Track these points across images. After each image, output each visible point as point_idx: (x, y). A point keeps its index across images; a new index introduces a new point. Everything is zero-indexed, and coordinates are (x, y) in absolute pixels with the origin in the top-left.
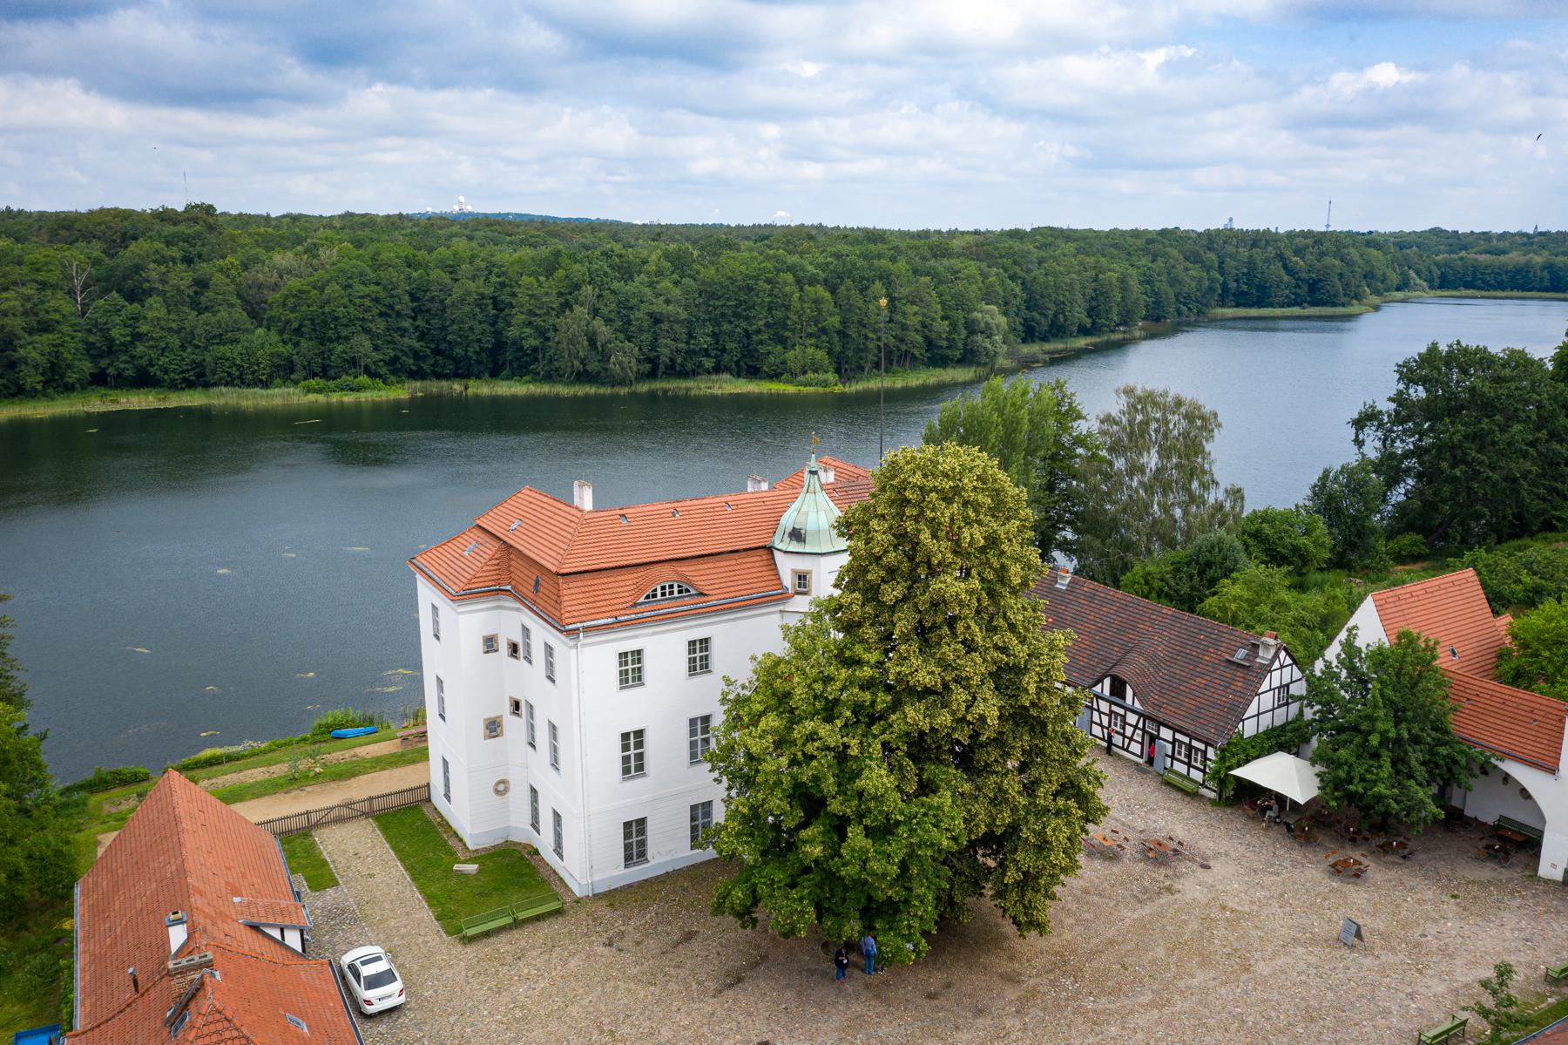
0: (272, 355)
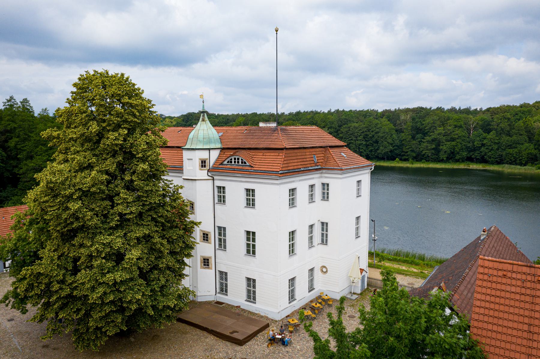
0: (528, 154)
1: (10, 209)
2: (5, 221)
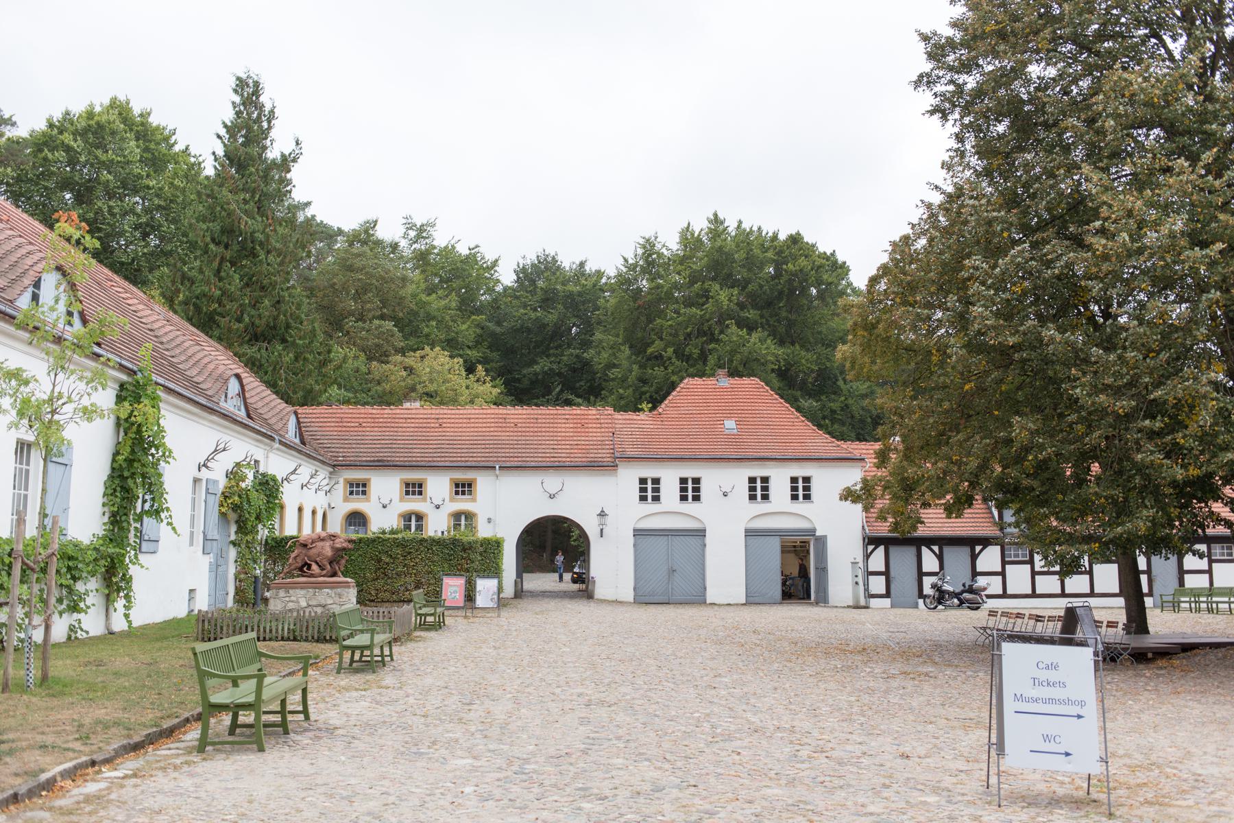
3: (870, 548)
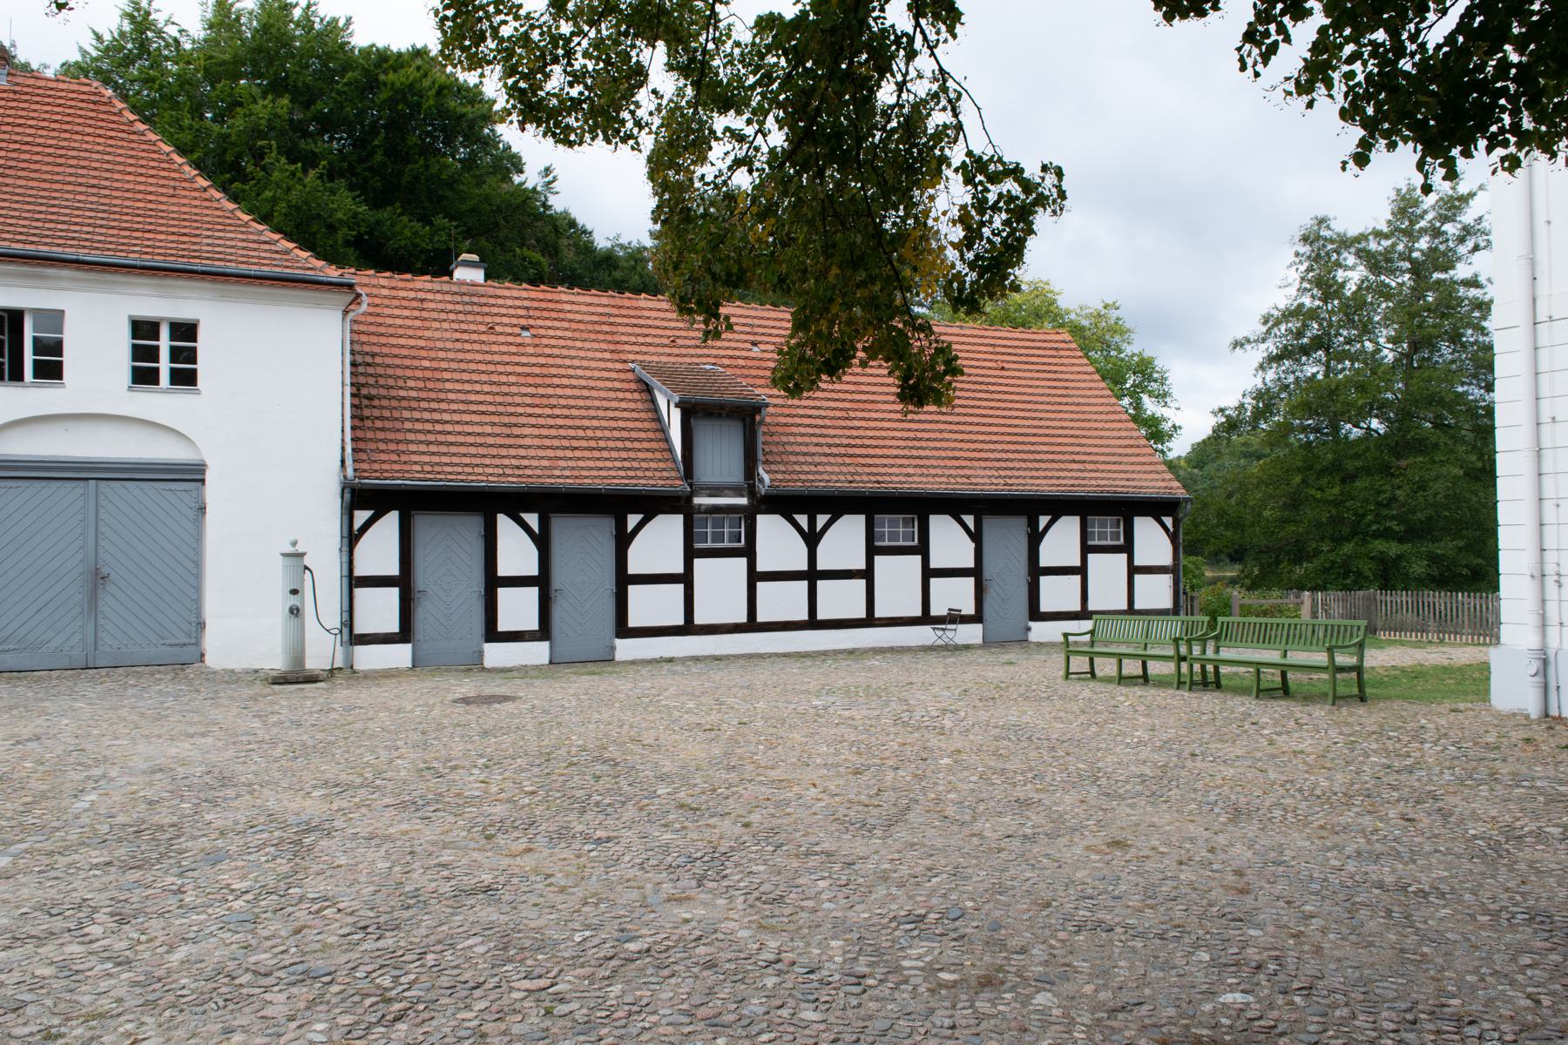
1: (573, 298)
2: (531, 350)
3: (361, 516)
